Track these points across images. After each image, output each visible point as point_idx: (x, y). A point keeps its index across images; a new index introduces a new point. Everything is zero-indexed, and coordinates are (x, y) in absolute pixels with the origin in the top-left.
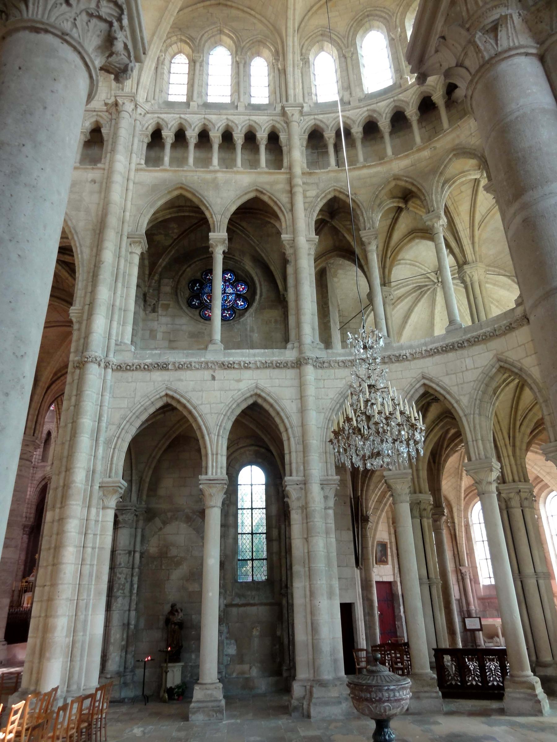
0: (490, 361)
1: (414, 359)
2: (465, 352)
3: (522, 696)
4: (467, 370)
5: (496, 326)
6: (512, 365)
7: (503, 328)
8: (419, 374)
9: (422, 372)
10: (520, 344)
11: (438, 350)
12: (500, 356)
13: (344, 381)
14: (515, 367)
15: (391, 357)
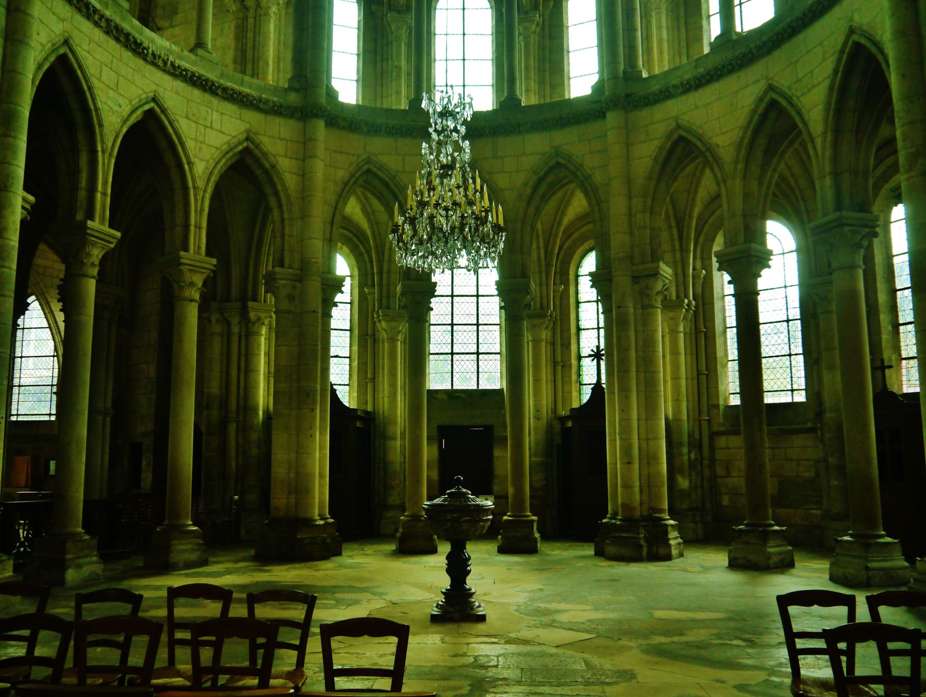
0: (239, 134)
1: (154, 64)
2: (215, 101)
3: (189, 546)
4: (211, 127)
5: (263, 96)
6: (263, 155)
7: (271, 104)
8: (151, 92)
9: (155, 91)
10: (282, 136)
11: (187, 74)
12: (253, 136)
13: (61, 26)
14: (267, 160)
15: (130, 37)
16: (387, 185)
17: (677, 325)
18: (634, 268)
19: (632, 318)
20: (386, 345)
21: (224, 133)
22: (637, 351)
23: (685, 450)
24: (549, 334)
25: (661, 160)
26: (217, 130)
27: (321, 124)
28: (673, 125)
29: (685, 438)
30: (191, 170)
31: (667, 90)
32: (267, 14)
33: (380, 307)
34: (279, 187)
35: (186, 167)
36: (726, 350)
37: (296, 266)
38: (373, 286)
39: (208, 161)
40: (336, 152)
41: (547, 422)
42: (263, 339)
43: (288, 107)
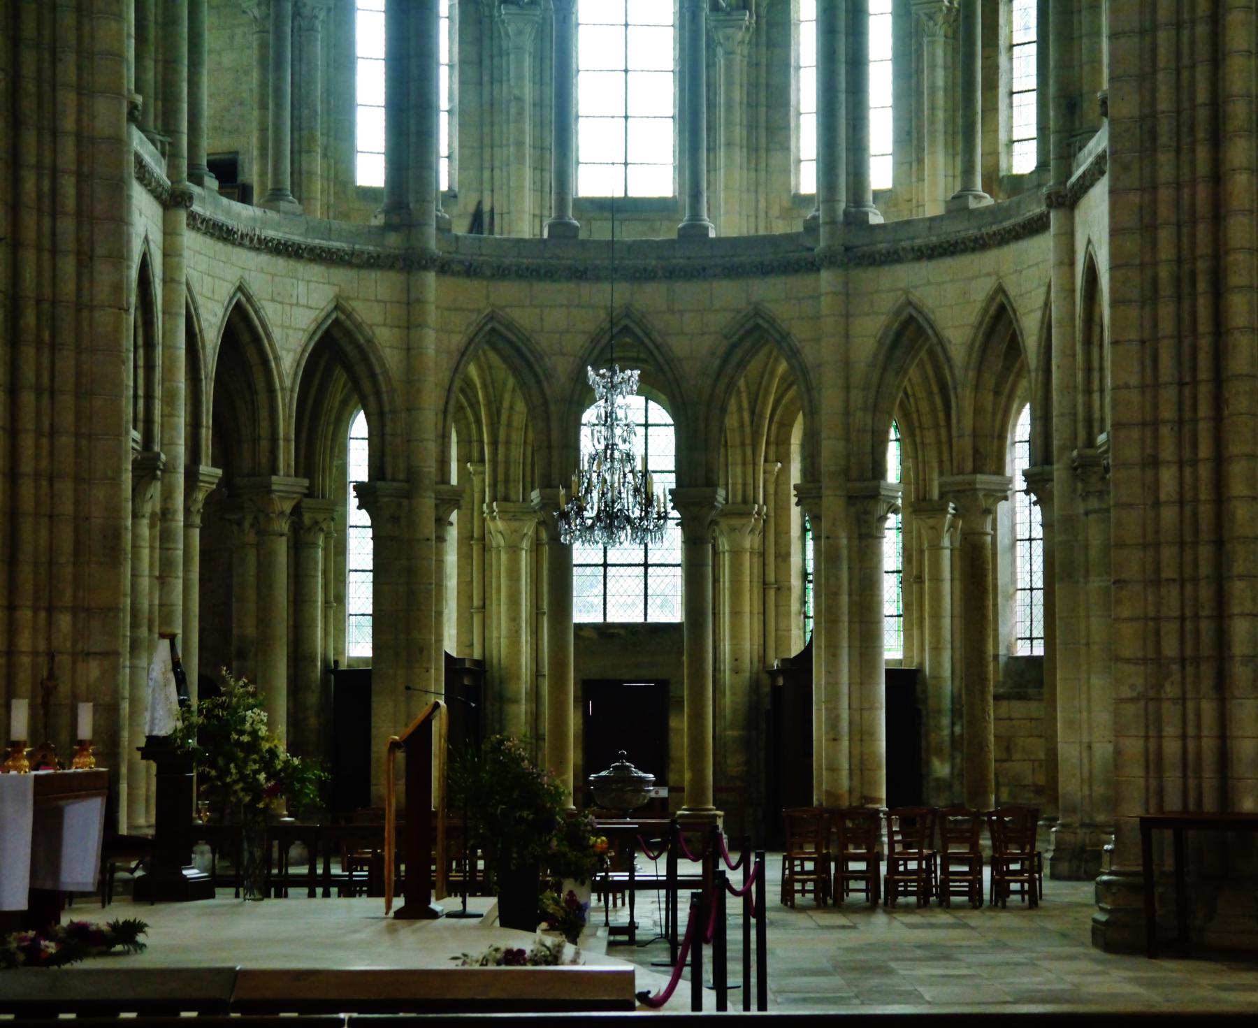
4: (297, 304)
5: (357, 247)
7: (366, 256)
12: (343, 302)
16: (518, 350)
17: (939, 537)
18: (849, 485)
19: (844, 552)
20: (504, 556)
21: (311, 308)
22: (850, 595)
23: (946, 721)
24: (757, 540)
25: (888, 342)
26: (303, 306)
27: (431, 278)
28: (903, 299)
29: (947, 704)
30: (278, 365)
31: (896, 252)
32: (312, 29)
33: (494, 499)
34: (378, 370)
35: (273, 364)
36: (1014, 573)
37: (402, 476)
38: (482, 461)
39: (295, 351)
40: (448, 309)
41: (751, 677)
42: (320, 553)
43: (388, 256)
